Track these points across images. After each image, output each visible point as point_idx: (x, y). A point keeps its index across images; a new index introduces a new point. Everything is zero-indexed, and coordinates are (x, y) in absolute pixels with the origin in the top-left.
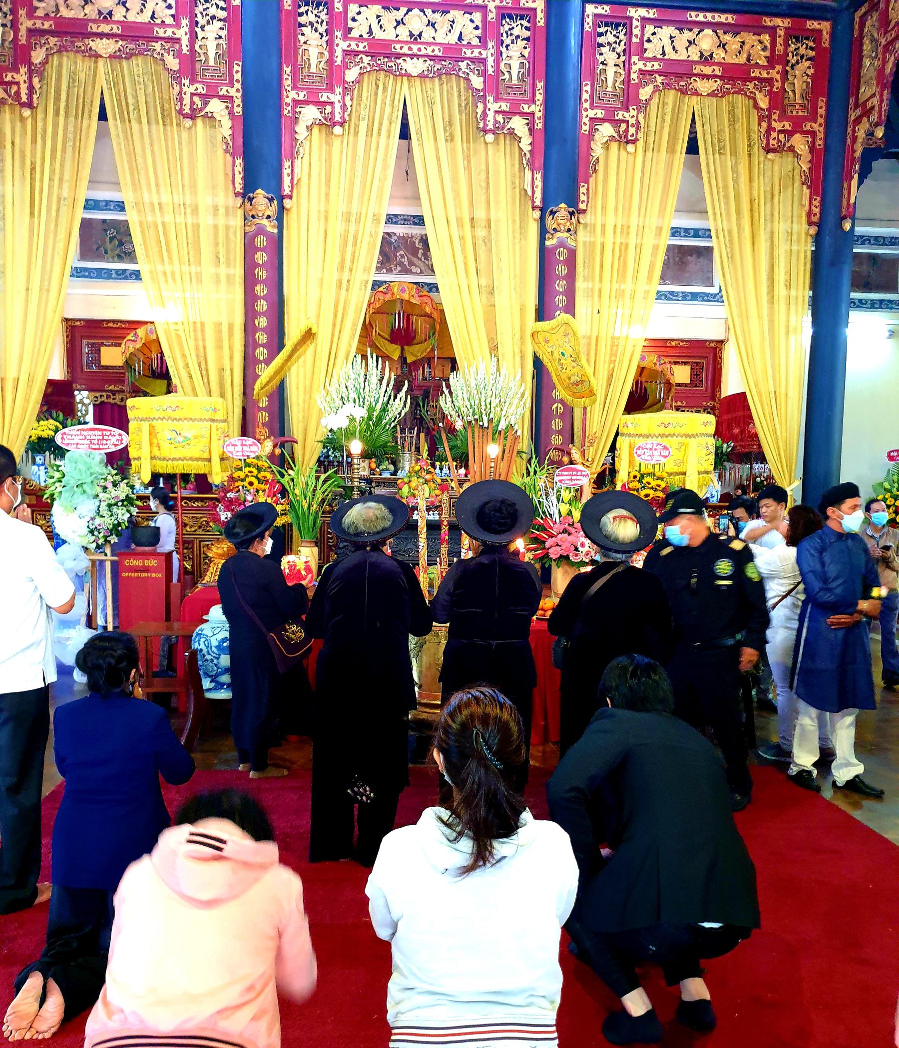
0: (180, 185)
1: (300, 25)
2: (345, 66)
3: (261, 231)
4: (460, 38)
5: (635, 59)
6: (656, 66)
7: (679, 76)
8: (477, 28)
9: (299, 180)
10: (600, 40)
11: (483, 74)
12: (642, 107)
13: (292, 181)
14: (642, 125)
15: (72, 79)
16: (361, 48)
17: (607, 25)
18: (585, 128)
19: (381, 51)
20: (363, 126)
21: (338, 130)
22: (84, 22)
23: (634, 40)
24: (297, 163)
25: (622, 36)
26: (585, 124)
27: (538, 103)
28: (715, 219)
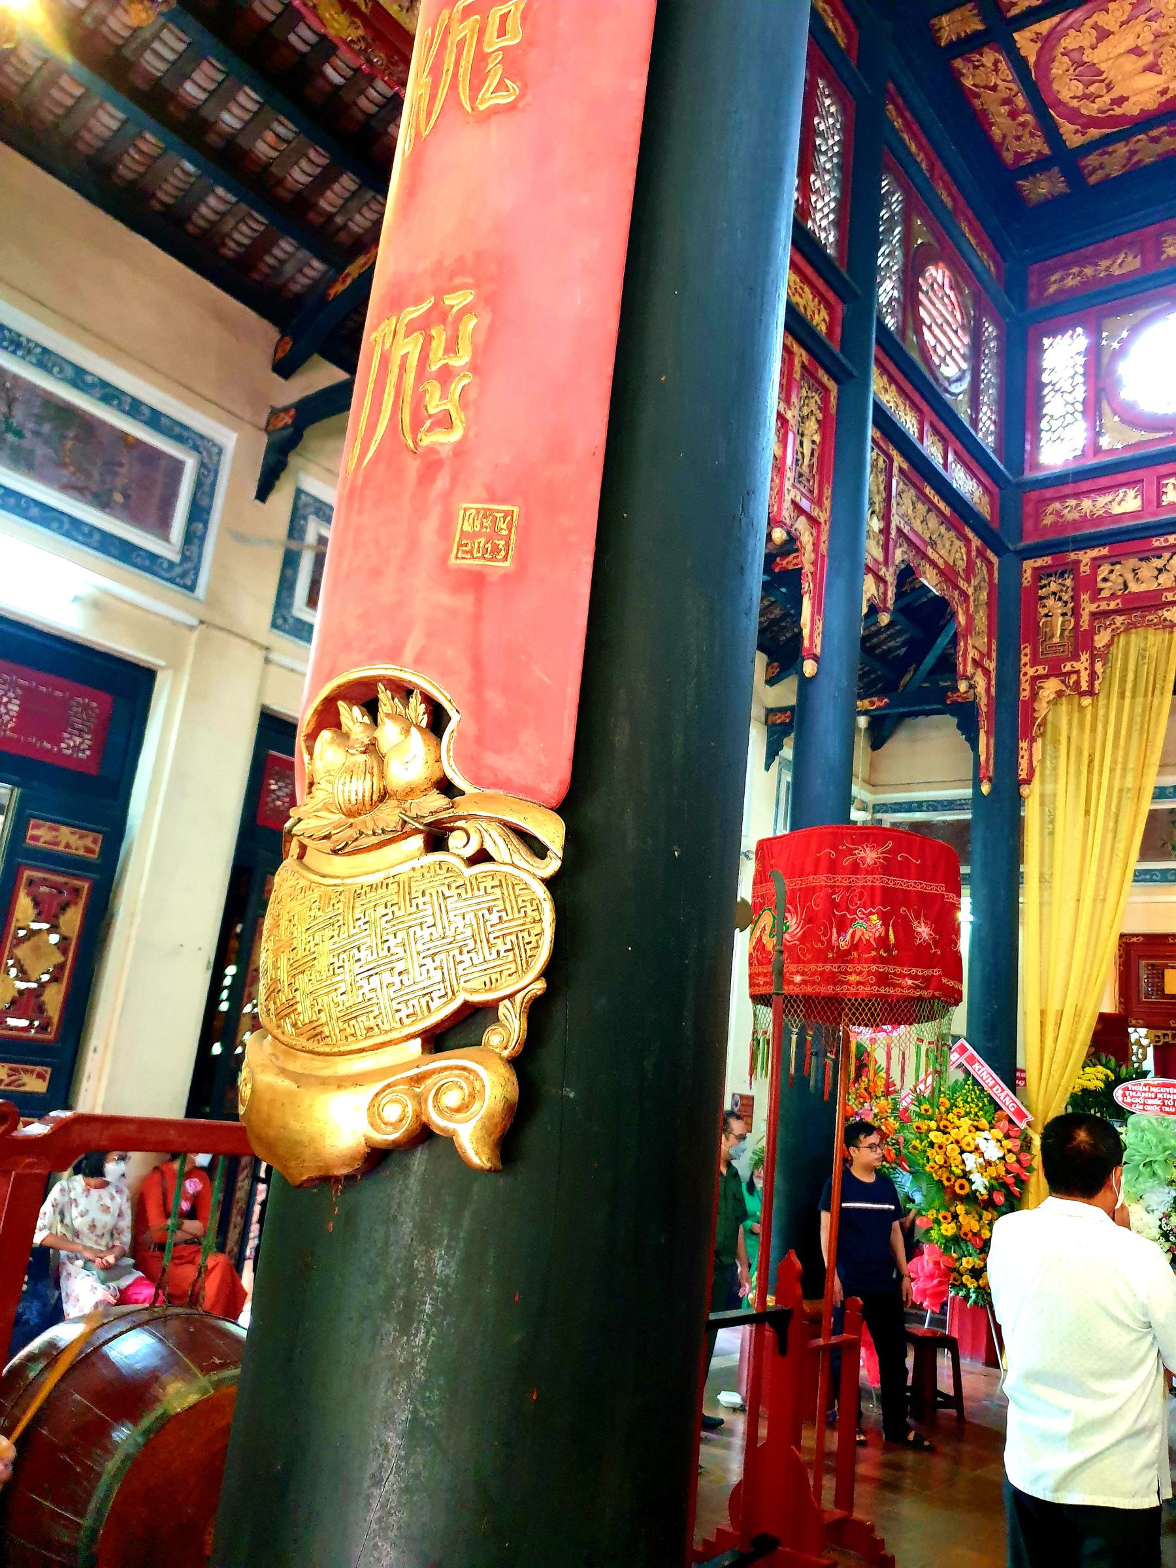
15: (1141, 656)
22: (1159, 592)
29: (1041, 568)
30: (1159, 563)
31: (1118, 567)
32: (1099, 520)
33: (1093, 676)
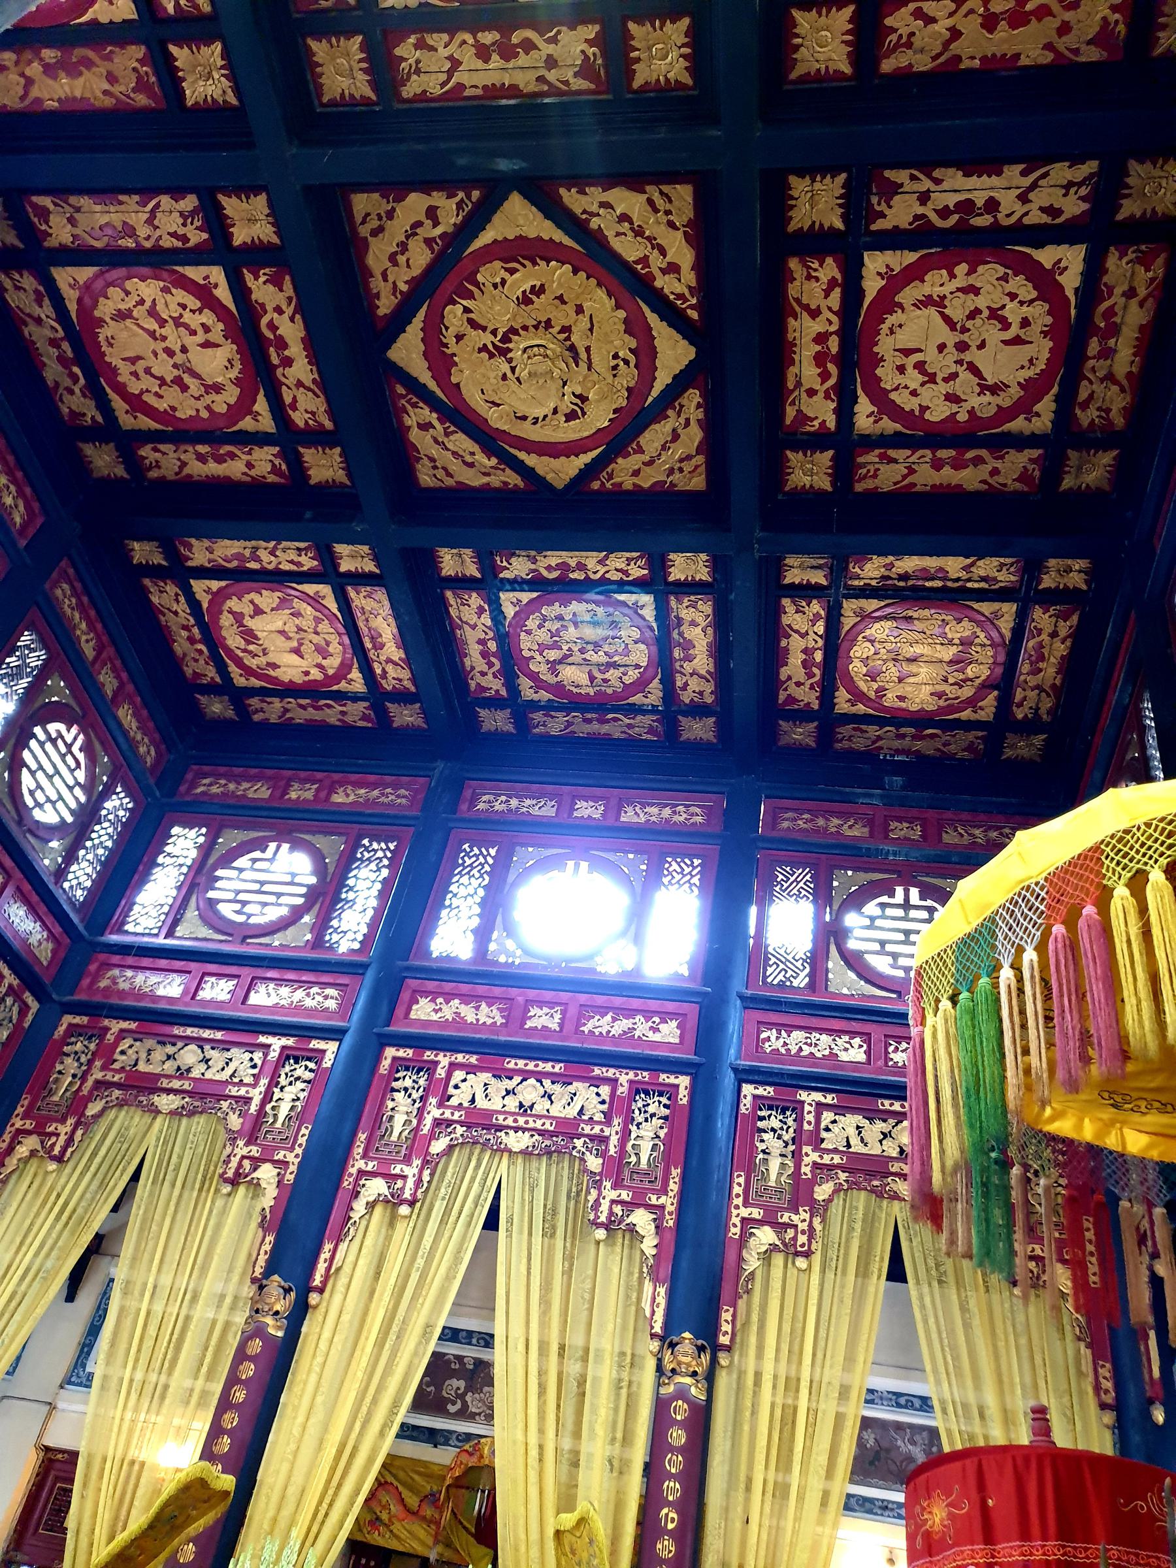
0: (196, 1265)
1: (393, 1090)
2: (432, 1136)
3: (259, 1332)
4: (581, 1112)
5: (806, 1149)
6: (837, 1160)
7: (871, 1174)
8: (603, 1102)
9: (338, 1269)
10: (760, 1124)
11: (602, 1154)
12: (819, 1209)
13: (328, 1269)
14: (818, 1233)
16: (456, 1117)
17: (770, 1108)
18: (735, 1232)
19: (480, 1122)
20: (439, 1207)
21: (404, 1210)
22: (157, 1077)
23: (806, 1127)
24: (343, 1247)
25: (790, 1122)
26: (735, 1226)
27: (671, 1194)
28: (938, 1382)
29: (77, 1025)
30: (170, 1049)
31: (138, 1044)
32: (142, 996)
33: (70, 1141)
